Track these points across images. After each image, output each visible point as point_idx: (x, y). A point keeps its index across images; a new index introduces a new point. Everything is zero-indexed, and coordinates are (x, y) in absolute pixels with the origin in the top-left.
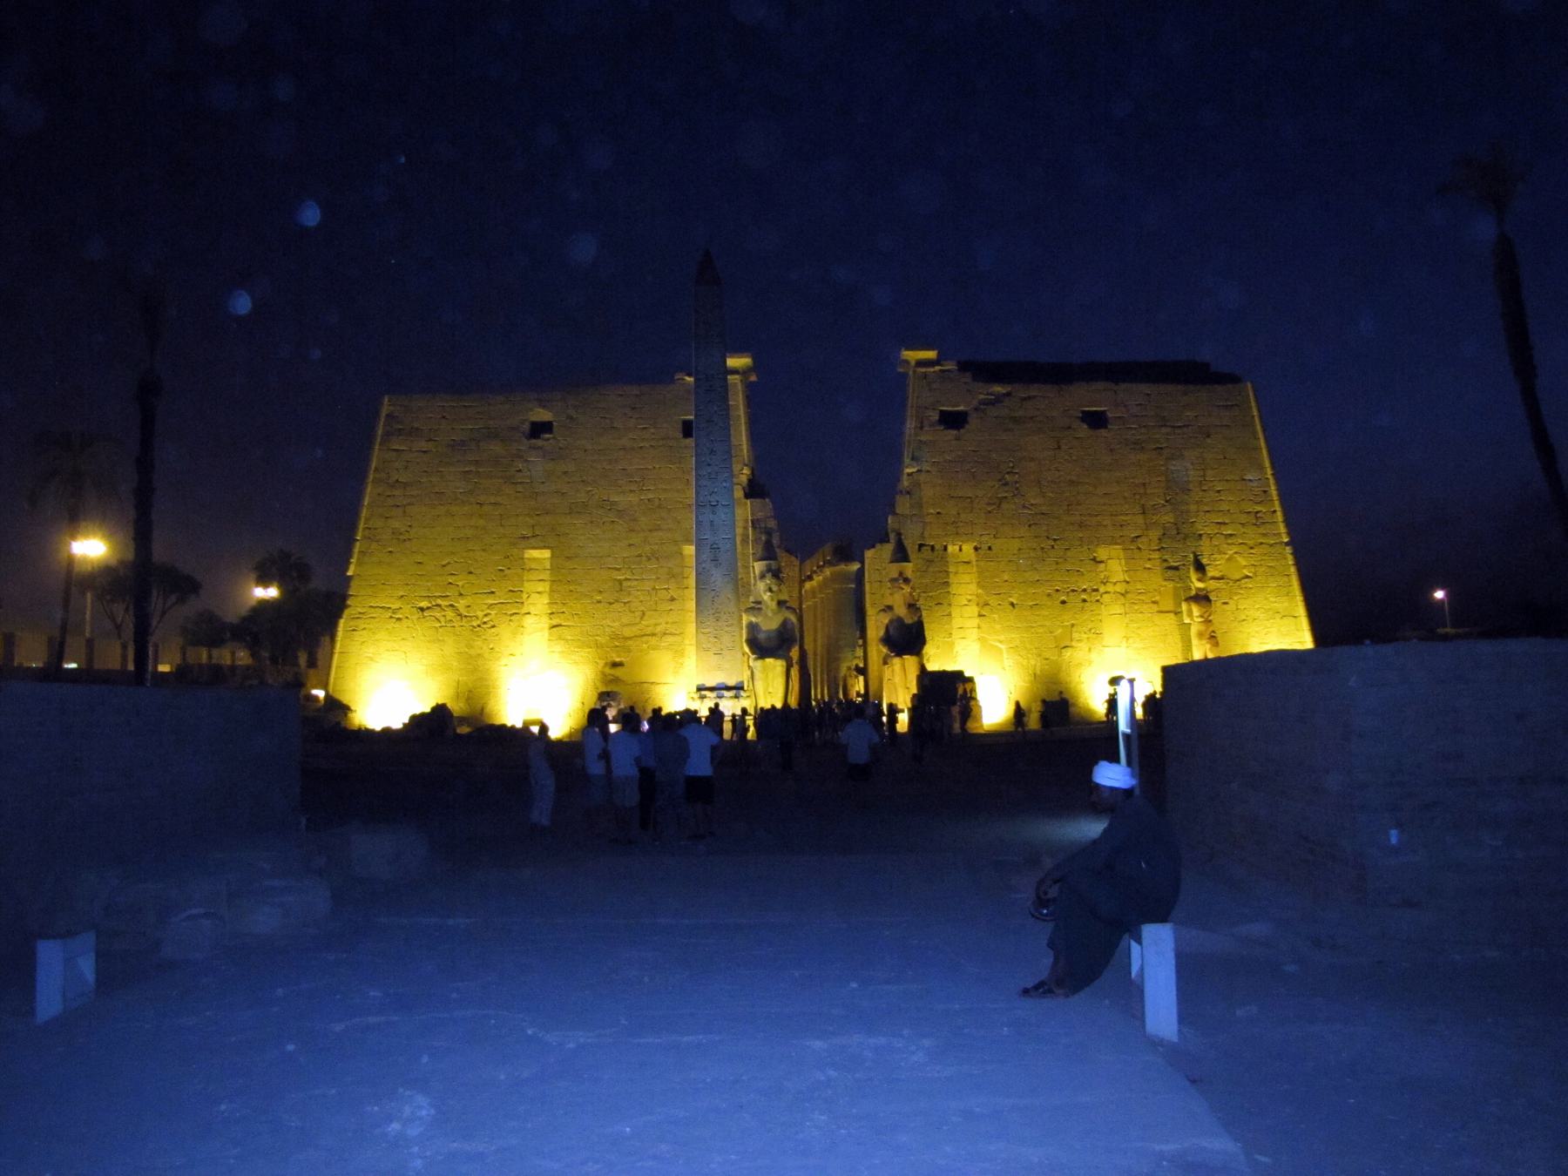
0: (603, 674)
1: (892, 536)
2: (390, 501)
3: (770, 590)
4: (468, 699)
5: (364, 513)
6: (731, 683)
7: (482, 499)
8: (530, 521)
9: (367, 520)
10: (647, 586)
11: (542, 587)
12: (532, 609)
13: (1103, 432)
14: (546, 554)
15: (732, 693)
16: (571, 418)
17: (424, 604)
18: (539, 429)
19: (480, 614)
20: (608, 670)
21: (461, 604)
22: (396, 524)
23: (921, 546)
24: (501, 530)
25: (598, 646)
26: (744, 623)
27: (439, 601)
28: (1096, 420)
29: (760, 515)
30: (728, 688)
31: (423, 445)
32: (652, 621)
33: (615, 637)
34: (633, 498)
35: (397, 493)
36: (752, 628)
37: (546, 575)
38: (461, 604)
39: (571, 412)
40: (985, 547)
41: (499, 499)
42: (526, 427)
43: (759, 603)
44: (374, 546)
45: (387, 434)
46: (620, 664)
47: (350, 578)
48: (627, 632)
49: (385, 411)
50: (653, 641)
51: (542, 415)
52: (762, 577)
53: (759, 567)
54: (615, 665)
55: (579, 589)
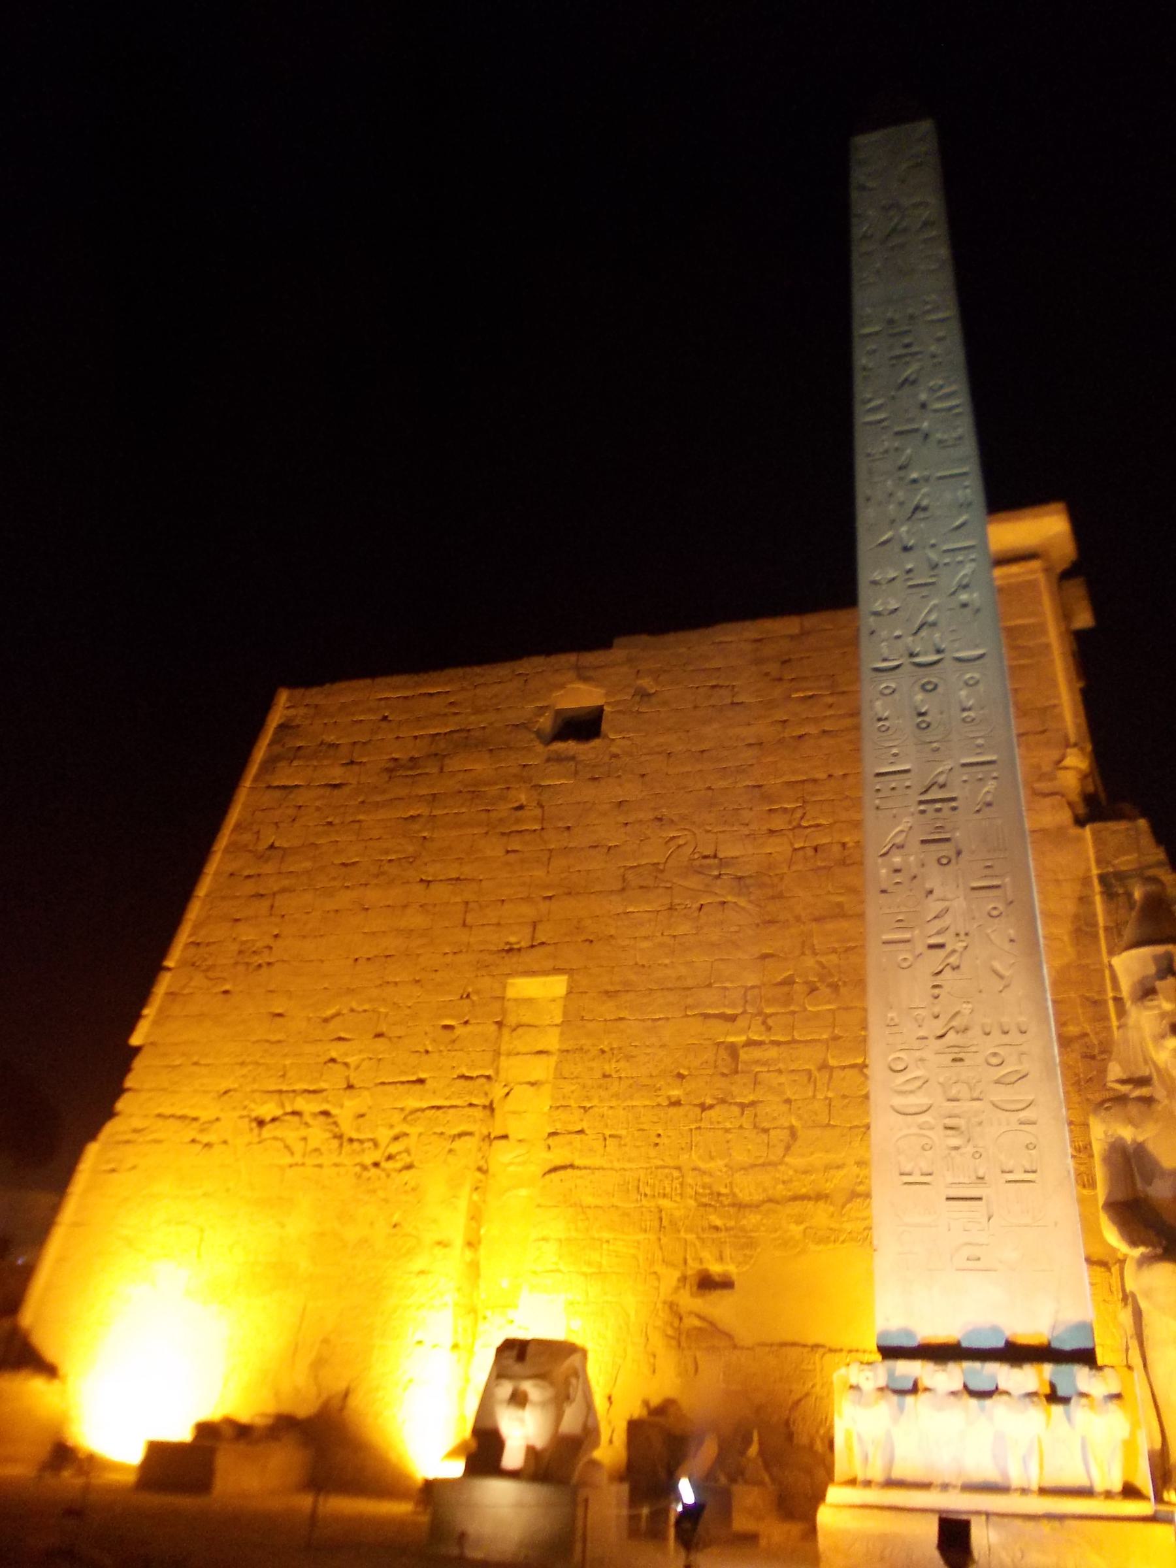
0: (672, 1307)
2: (249, 887)
4: (318, 1364)
5: (194, 911)
6: (1032, 1327)
7: (430, 872)
8: (528, 911)
9: (197, 927)
10: (807, 1059)
11: (541, 1069)
12: (514, 1128)
14: (557, 985)
15: (1028, 1378)
16: (643, 695)
17: (268, 1110)
18: (583, 726)
19: (383, 1135)
20: (689, 1301)
21: (346, 1110)
22: (247, 933)
24: (463, 936)
25: (663, 1224)
26: (1098, 1148)
27: (301, 1104)
29: (1126, 862)
30: (1015, 1354)
31: (337, 773)
32: (819, 1158)
33: (711, 1200)
34: (778, 848)
35: (268, 868)
36: (1130, 1163)
37: (552, 1041)
38: (346, 1110)
39: (646, 683)
41: (467, 871)
42: (546, 722)
43: (1144, 1081)
44: (199, 980)
45: (270, 764)
46: (726, 1284)
47: (137, 1050)
48: (748, 1188)
49: (275, 719)
50: (821, 1215)
51: (581, 696)
52: (1146, 992)
53: (1130, 965)
54: (707, 1283)
55: (625, 1068)
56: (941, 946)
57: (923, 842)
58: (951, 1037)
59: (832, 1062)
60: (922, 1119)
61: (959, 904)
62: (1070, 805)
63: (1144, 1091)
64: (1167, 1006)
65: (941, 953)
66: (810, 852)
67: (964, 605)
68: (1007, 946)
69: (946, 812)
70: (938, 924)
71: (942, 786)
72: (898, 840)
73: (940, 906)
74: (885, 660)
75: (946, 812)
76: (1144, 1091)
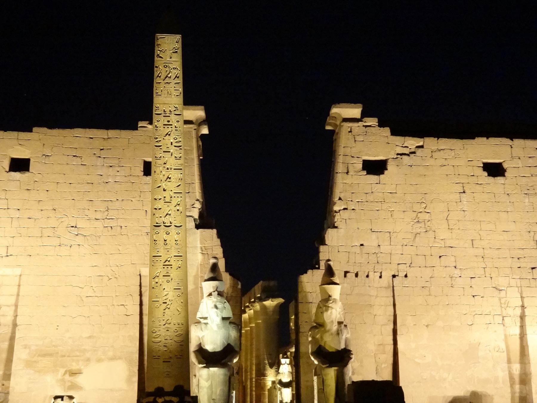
1: (322, 264)
3: (216, 307)
13: (500, 180)
23: (346, 273)
28: (495, 170)
29: (208, 244)
34: (99, 225)
40: (402, 274)
56: (166, 303)
57: (164, 276)
58: (167, 325)
59: (115, 304)
60: (158, 344)
61: (171, 293)
62: (195, 220)
63: (205, 321)
64: (215, 300)
65: (166, 305)
66: (110, 228)
67: (178, 210)
68: (181, 304)
69: (169, 268)
70: (165, 298)
71: (169, 261)
72: (157, 275)
73: (167, 293)
74: (157, 223)
75: (169, 268)
76: (205, 321)
